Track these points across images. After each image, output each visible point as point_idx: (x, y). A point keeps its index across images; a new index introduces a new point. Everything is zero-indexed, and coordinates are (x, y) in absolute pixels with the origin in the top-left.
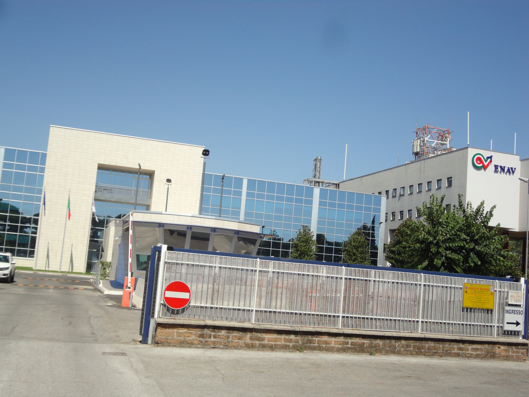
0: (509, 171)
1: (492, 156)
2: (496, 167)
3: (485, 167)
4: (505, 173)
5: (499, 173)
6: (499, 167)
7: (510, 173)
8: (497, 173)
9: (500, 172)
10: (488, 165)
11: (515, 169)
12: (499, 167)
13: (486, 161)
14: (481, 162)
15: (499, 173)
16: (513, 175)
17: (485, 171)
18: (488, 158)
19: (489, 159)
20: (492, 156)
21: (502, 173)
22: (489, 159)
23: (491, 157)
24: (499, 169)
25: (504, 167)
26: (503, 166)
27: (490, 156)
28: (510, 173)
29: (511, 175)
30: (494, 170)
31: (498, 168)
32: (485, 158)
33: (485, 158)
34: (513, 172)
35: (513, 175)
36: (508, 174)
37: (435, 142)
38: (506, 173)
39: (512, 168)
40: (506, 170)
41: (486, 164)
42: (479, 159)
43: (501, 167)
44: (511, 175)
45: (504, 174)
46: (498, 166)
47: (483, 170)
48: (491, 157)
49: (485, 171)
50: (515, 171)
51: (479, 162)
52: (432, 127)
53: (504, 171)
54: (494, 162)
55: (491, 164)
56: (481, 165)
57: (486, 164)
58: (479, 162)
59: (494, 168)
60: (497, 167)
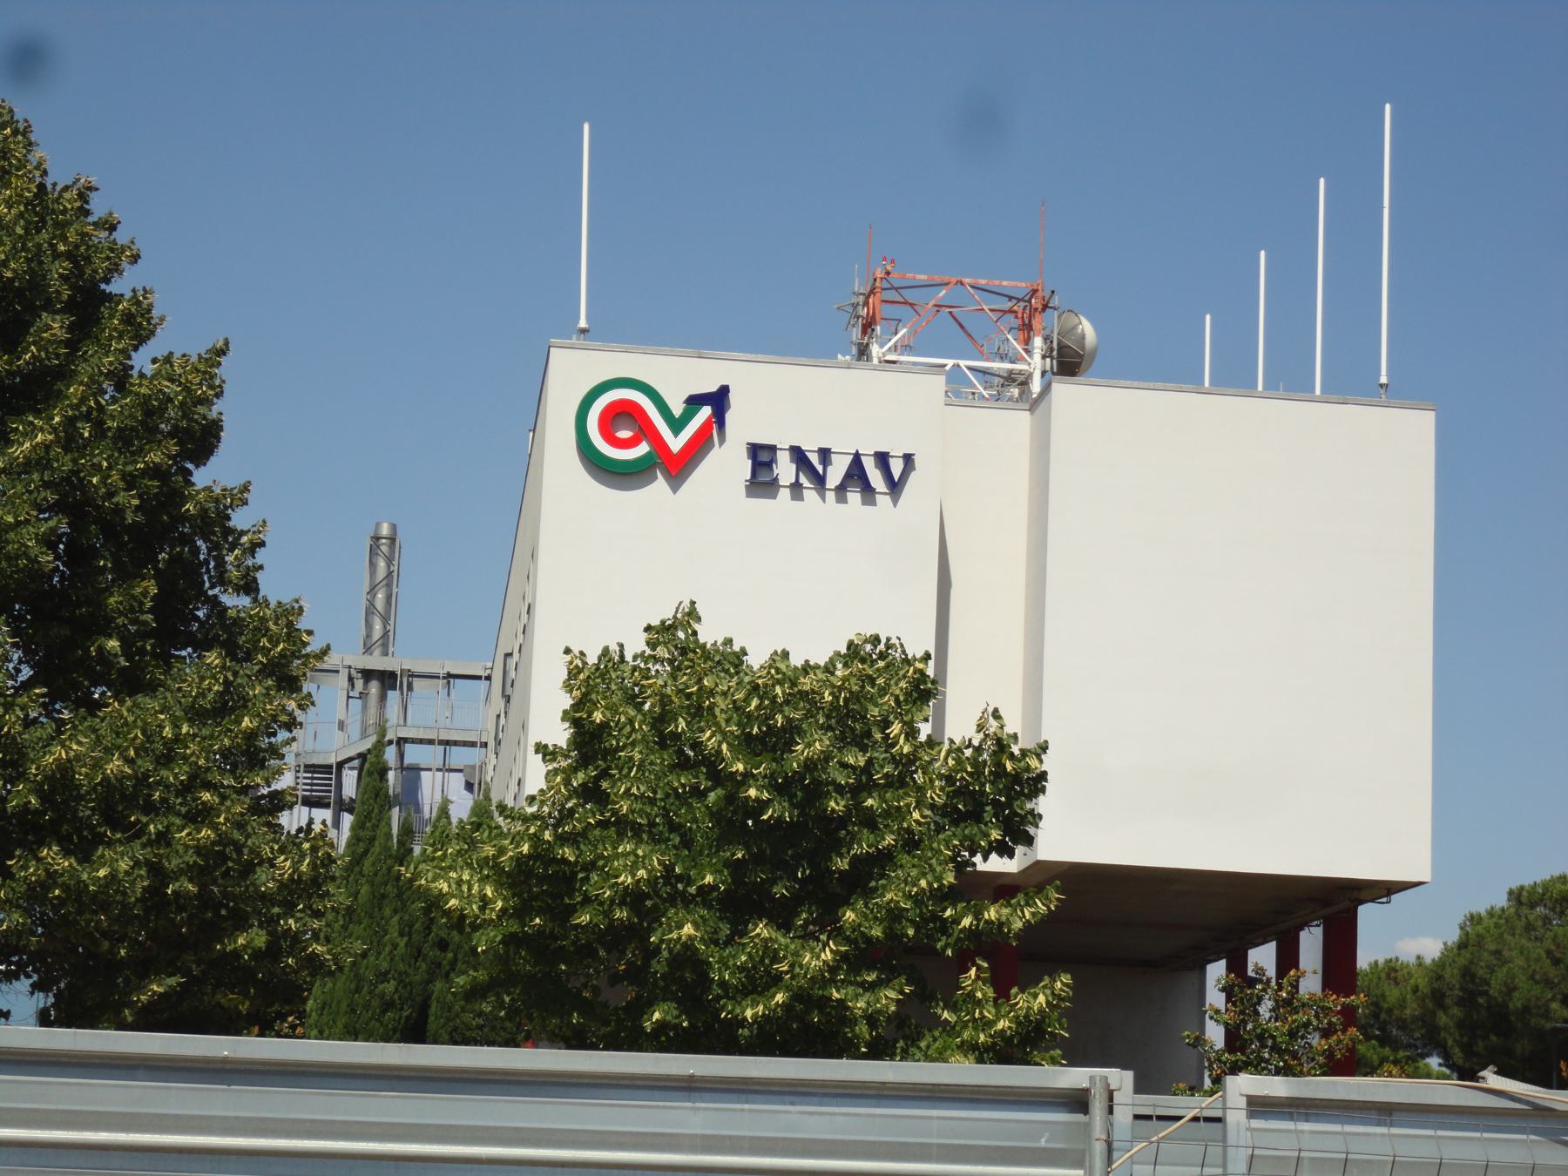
0: (855, 472)
1: (724, 391)
2: (761, 456)
3: (677, 467)
4: (831, 496)
5: (784, 494)
6: (783, 459)
7: (868, 490)
8: (774, 497)
9: (796, 487)
10: (699, 446)
11: (908, 459)
12: (783, 459)
13: (677, 425)
14: (646, 430)
15: (784, 494)
16: (895, 503)
17: (675, 489)
18: (695, 401)
19: (706, 412)
20: (724, 391)
21: (810, 495)
22: (706, 412)
23: (719, 400)
24: (785, 470)
25: (825, 454)
26: (810, 446)
27: (713, 388)
28: (868, 490)
29: (884, 501)
30: (749, 478)
31: (769, 465)
32: (677, 409)
33: (677, 409)
34: (895, 487)
35: (895, 503)
36: (854, 497)
37: (945, 365)
38: (841, 489)
39: (882, 459)
40: (835, 475)
41: (676, 443)
42: (621, 413)
43: (798, 455)
44: (884, 501)
45: (823, 499)
46: (772, 449)
47: (660, 484)
48: (719, 400)
49: (675, 489)
50: (913, 478)
51: (624, 434)
52: (922, 277)
53: (819, 480)
54: (743, 426)
55: (722, 440)
56: (643, 448)
57: (676, 443)
58: (624, 434)
59: (750, 462)
60: (764, 457)
